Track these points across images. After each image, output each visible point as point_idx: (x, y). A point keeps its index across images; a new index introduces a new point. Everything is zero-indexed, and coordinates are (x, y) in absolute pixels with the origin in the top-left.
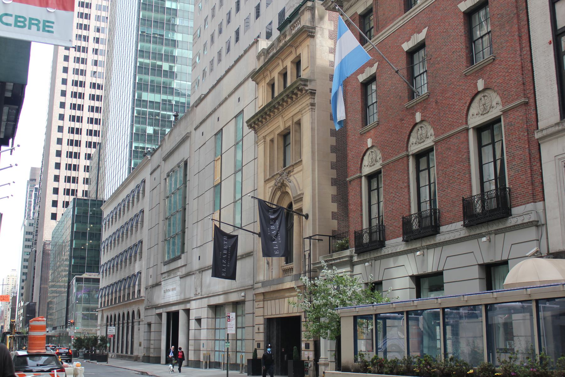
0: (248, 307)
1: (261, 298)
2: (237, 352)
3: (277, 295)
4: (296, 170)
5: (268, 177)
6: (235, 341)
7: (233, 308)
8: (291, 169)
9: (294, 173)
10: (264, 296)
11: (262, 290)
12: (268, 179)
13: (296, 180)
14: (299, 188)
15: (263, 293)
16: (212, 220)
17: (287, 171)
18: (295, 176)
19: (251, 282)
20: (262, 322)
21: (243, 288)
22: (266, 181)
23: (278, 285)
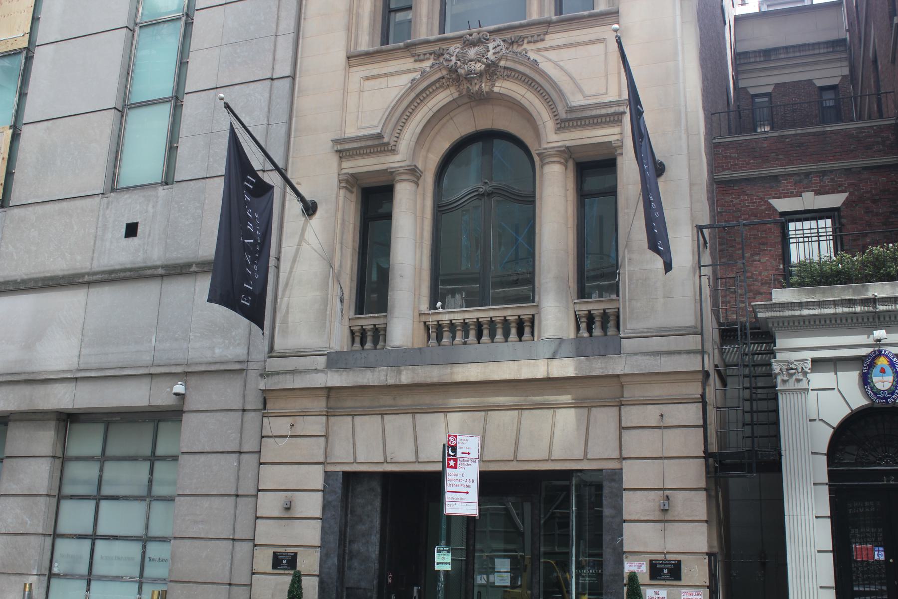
0: (194, 432)
1: (320, 404)
2: (51, 575)
3: (426, 399)
4: (555, 39)
5: (364, 46)
6: (49, 540)
7: (57, 431)
8: (534, 31)
9: (540, 45)
10: (328, 397)
11: (335, 380)
12: (367, 54)
13: (562, 69)
14: (581, 91)
15: (330, 389)
16: (227, 106)
17: (507, 36)
18: (551, 55)
19: (239, 352)
20: (319, 484)
21: (179, 370)
22: (354, 58)
23: (448, 370)
